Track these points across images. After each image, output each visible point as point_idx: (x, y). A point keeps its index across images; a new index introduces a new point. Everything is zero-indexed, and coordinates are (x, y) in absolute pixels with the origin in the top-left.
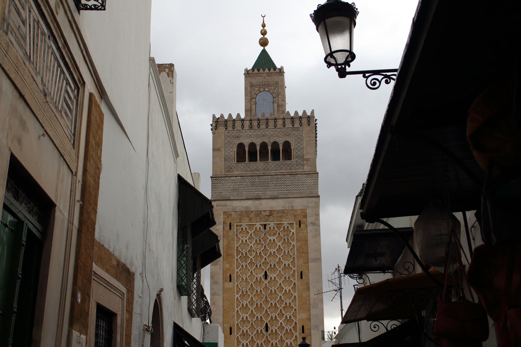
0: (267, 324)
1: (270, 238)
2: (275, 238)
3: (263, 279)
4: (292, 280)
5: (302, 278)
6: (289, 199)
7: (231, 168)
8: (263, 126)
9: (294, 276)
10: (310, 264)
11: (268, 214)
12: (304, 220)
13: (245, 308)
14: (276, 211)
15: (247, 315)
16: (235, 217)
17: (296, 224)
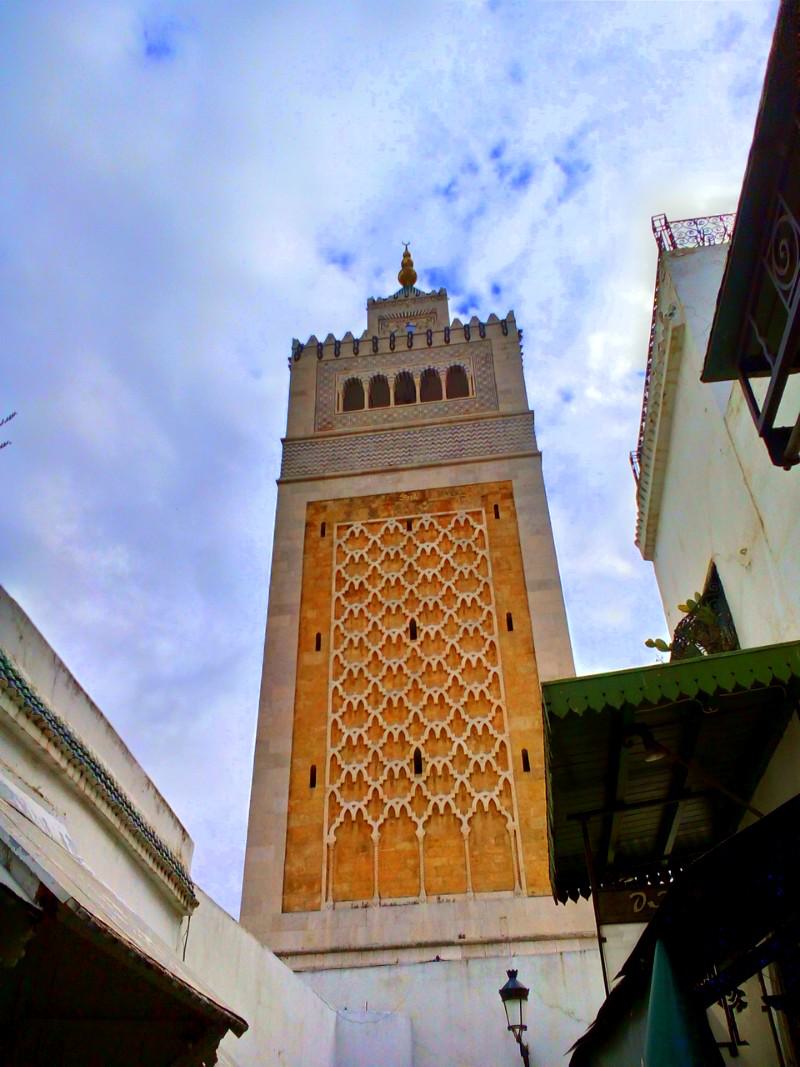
0: (418, 753)
1: (421, 546)
4: (486, 635)
5: (510, 628)
7: (329, 423)
8: (401, 346)
9: (490, 626)
10: (531, 595)
12: (508, 503)
13: (355, 713)
15: (362, 731)
17: (486, 512)
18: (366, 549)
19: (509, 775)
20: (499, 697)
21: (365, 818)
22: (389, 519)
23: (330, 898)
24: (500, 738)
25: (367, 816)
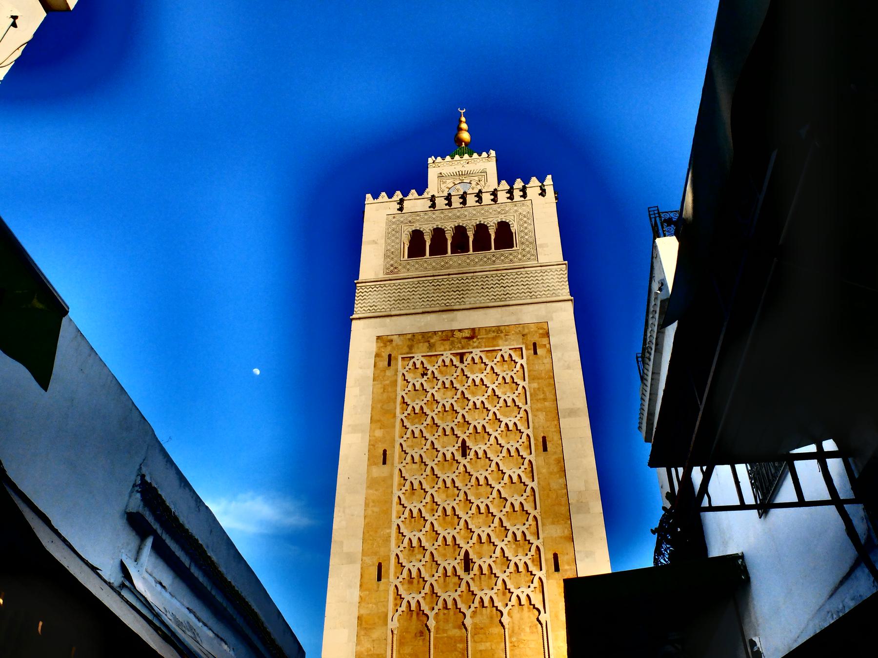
3: (458, 456)
6: (511, 308)
12: (545, 341)
17: (527, 349)
19: (542, 574)
22: (444, 353)
25: (425, 607)
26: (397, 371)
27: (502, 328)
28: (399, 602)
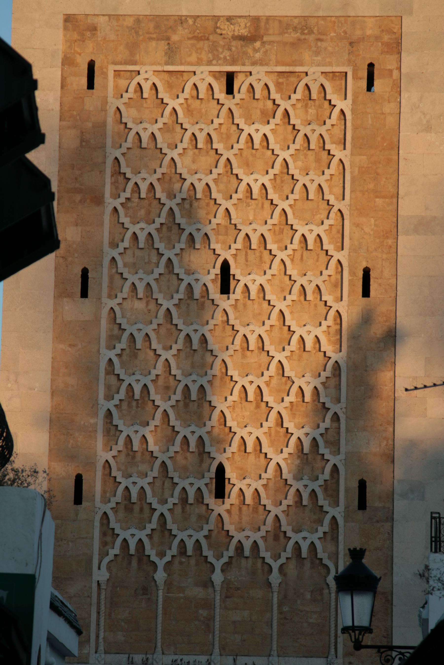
2: (266, 129)
10: (401, 238)
11: (244, 32)
14: (279, 20)
16: (112, 37)
17: (355, 77)
18: (160, 125)
19: (337, 512)
20: (338, 400)
21: (147, 553)
23: (101, 648)
24: (333, 460)
25: (150, 551)
26: (105, 101)
27: (312, 21)
28: (109, 539)
